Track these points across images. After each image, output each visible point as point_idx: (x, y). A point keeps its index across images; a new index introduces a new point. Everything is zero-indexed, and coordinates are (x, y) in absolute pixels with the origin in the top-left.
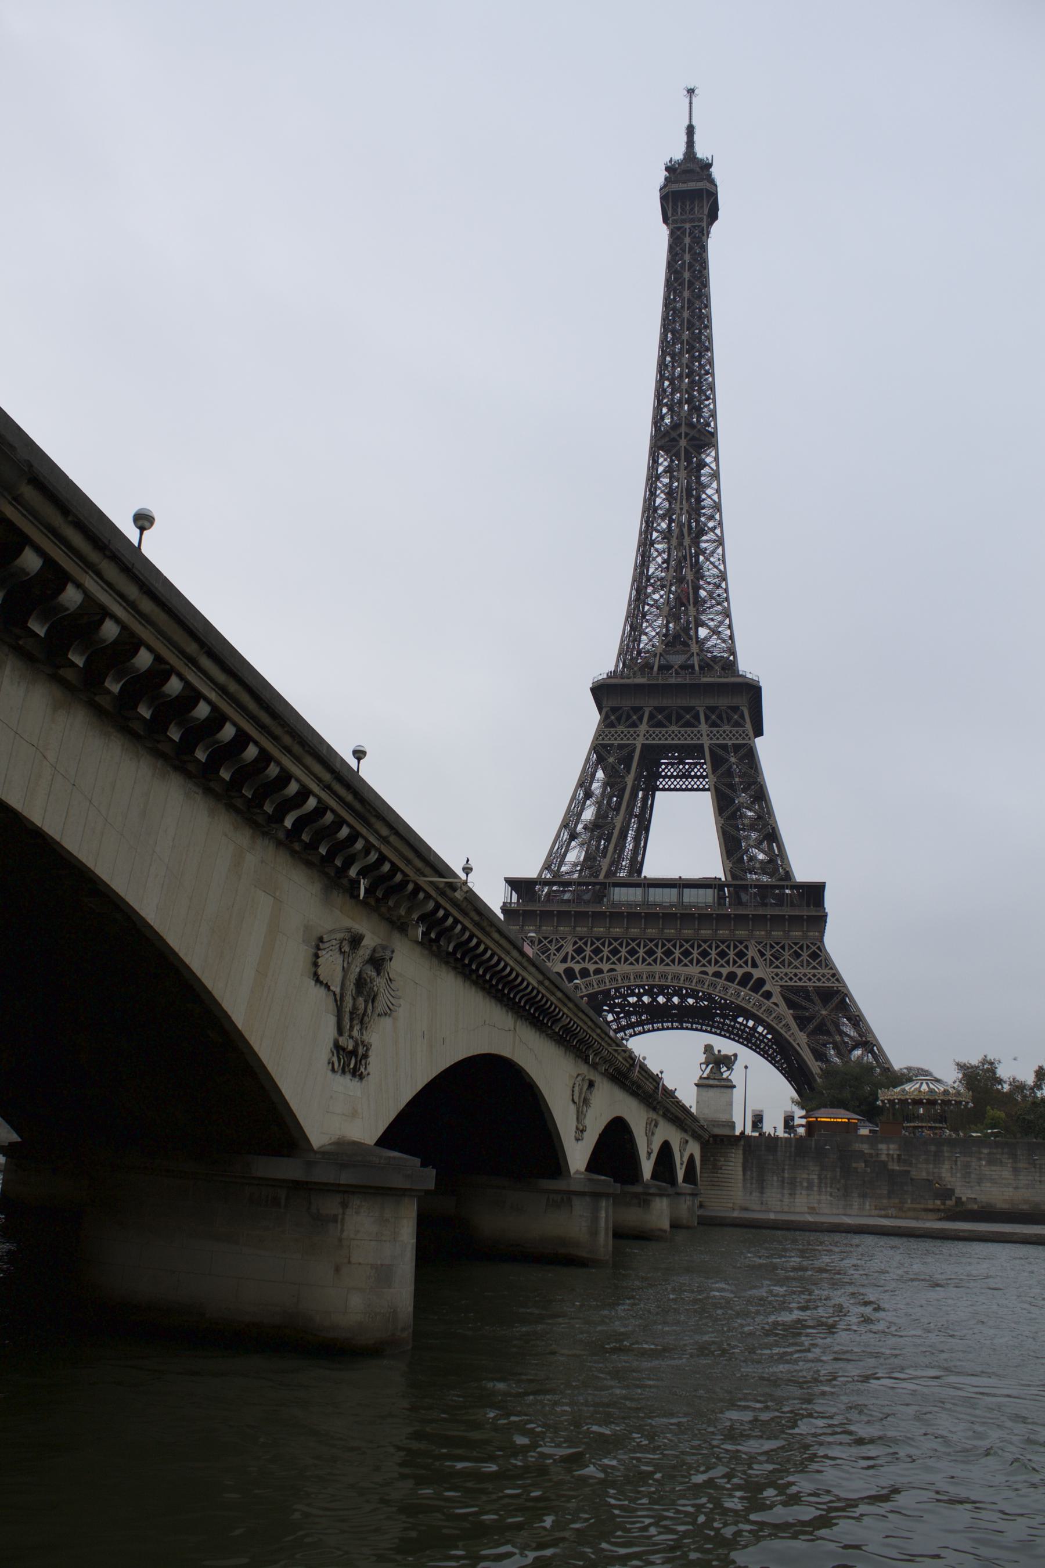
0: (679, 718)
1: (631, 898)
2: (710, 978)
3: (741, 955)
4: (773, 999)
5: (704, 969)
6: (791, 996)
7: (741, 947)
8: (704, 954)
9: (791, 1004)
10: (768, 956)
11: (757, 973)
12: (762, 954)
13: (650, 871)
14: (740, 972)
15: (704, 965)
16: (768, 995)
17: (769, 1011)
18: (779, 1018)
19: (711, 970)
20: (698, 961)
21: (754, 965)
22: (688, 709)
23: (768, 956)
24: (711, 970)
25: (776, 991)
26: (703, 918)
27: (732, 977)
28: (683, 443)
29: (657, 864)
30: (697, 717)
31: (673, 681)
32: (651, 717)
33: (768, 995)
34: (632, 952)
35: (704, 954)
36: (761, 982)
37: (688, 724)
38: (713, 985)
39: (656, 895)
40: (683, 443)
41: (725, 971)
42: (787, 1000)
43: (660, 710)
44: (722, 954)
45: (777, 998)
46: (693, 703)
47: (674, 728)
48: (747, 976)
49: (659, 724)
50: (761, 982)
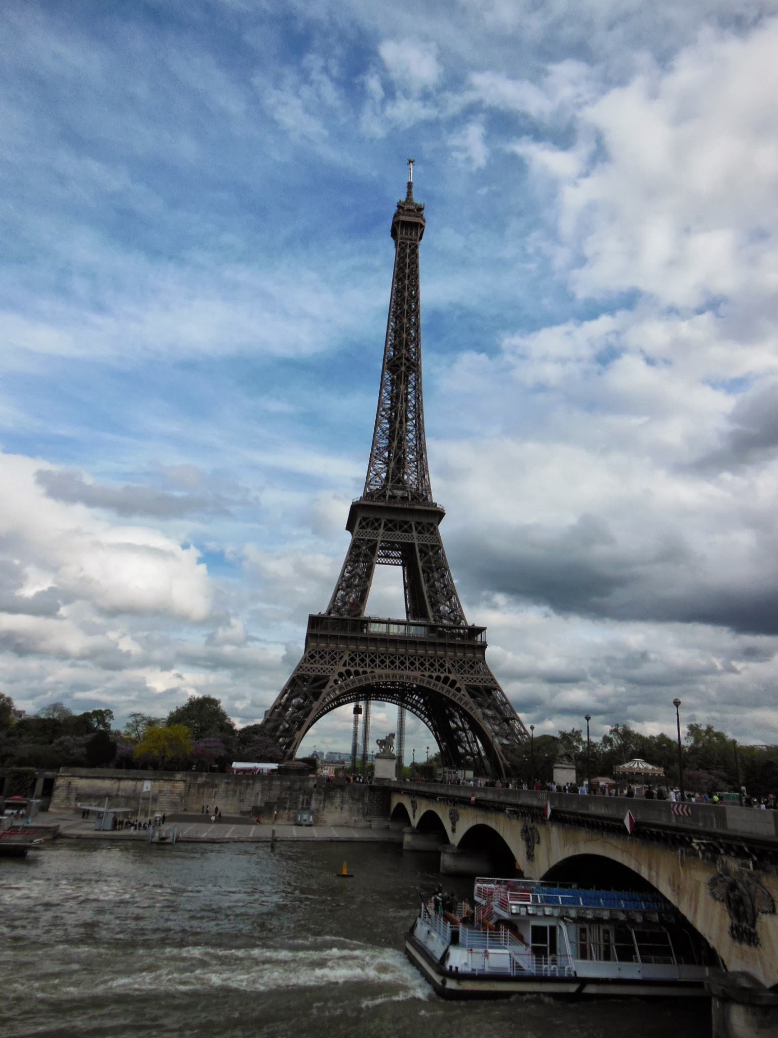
0: (401, 527)
1: (380, 630)
2: (426, 679)
3: (442, 666)
4: (462, 692)
7: (441, 661)
8: (422, 664)
10: (457, 666)
11: (452, 677)
12: (454, 666)
13: (403, 617)
14: (443, 676)
16: (459, 690)
17: (461, 699)
18: (466, 703)
19: (427, 674)
21: (450, 672)
22: (406, 523)
23: (457, 666)
24: (427, 674)
26: (423, 644)
27: (438, 678)
28: (403, 368)
29: (369, 610)
30: (410, 527)
31: (396, 505)
32: (386, 525)
33: (459, 690)
34: (382, 662)
35: (422, 664)
36: (454, 683)
37: (405, 531)
38: (429, 683)
39: (375, 629)
40: (403, 368)
41: (435, 675)
43: (390, 521)
44: (432, 665)
46: (408, 519)
47: (398, 532)
48: (447, 678)
49: (390, 530)
50: (454, 683)
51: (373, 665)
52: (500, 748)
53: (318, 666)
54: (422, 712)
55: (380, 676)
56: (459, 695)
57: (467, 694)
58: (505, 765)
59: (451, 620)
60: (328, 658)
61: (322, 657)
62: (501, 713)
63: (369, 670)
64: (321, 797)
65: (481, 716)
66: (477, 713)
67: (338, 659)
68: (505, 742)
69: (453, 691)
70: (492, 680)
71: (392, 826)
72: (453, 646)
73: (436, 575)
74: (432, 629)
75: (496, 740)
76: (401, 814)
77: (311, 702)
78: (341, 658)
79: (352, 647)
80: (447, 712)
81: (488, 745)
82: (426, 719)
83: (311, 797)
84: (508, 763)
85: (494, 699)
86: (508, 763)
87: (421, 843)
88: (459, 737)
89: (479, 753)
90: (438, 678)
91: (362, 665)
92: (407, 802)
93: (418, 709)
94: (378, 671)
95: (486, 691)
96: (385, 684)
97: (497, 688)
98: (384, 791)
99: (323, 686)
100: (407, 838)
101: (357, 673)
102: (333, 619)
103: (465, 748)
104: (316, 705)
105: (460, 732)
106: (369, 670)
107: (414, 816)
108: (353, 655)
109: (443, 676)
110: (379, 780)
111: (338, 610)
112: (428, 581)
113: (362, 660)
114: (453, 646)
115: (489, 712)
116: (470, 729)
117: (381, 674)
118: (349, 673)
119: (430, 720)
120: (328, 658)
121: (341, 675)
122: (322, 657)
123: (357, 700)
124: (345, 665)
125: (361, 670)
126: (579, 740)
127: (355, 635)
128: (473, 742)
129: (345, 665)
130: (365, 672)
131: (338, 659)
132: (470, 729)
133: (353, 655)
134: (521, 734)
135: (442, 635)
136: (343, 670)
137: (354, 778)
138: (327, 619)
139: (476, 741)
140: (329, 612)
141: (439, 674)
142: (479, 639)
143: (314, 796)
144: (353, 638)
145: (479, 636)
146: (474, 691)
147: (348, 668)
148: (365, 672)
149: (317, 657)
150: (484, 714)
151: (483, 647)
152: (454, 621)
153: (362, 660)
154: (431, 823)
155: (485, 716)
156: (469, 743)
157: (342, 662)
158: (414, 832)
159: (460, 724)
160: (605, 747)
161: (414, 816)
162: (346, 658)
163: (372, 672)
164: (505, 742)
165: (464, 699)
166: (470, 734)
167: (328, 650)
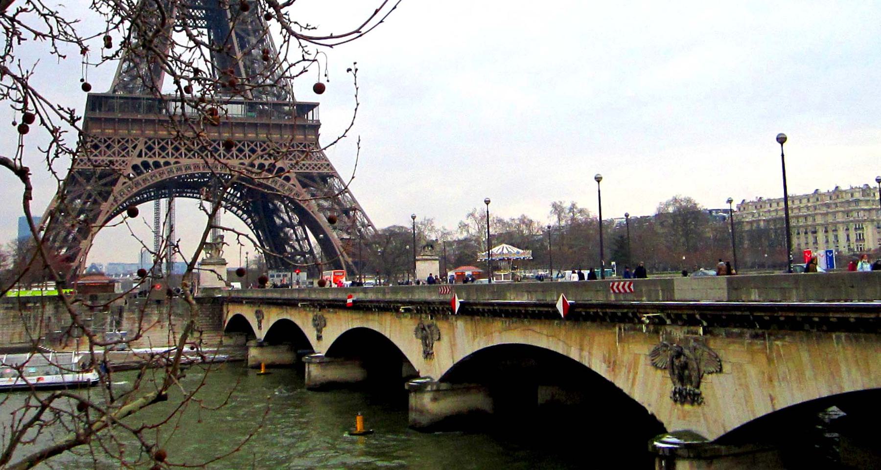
4: (292, 182)
5: (241, 161)
6: (303, 179)
9: (304, 186)
11: (279, 164)
14: (267, 163)
15: (241, 159)
17: (291, 190)
18: (297, 195)
19: (247, 161)
20: (237, 156)
24: (247, 161)
25: (292, 175)
26: (240, 125)
27: (261, 166)
36: (281, 170)
41: (257, 163)
42: (300, 181)
45: (293, 181)
51: (177, 154)
52: (340, 243)
53: (104, 158)
54: (239, 208)
55: (188, 168)
56: (288, 185)
57: (298, 184)
58: (346, 262)
59: (274, 95)
60: (117, 147)
61: (108, 147)
62: (339, 203)
63: (172, 160)
64: (136, 316)
65: (316, 209)
66: (312, 206)
67: (130, 149)
68: (346, 236)
69: (281, 180)
70: (328, 165)
71: (226, 341)
72: (279, 127)
73: (254, 41)
74: (251, 106)
75: (335, 234)
76: (240, 326)
77: (100, 204)
78: (134, 147)
79: (150, 132)
80: (271, 206)
81: (325, 243)
82: (245, 216)
83: (121, 316)
84: (350, 260)
85: (331, 188)
86: (350, 260)
87: (281, 355)
88: (286, 234)
89: (311, 252)
90: (261, 166)
91: (164, 154)
92: (249, 314)
93: (233, 204)
94: (184, 161)
95: (321, 179)
96: (192, 176)
97: (333, 175)
98: (214, 303)
99: (114, 182)
100: (254, 353)
101: (157, 165)
102: (121, 98)
103: (292, 247)
104: (105, 206)
105: (287, 229)
106: (172, 160)
107: (260, 328)
108: (150, 143)
109: (267, 163)
110: (206, 290)
111: (125, 87)
112: (242, 47)
113: (163, 149)
114: (279, 127)
115: (326, 204)
116: (300, 224)
117: (189, 164)
118: (146, 165)
119: (249, 216)
120: (117, 147)
121: (135, 167)
122: (108, 147)
123: (157, 197)
124: (140, 155)
125: (162, 161)
126: (432, 229)
127: (152, 117)
128: (303, 239)
129: (140, 155)
130: (167, 164)
131: (130, 149)
132: (300, 224)
133: (150, 143)
134: (363, 225)
135: (262, 113)
136: (138, 161)
137: (160, 288)
138: (113, 98)
139: (307, 238)
140: (115, 91)
141: (262, 161)
142: (310, 118)
143: (125, 315)
144: (148, 121)
145: (310, 113)
146: (307, 180)
147: (144, 159)
148: (167, 164)
149: (103, 147)
150: (318, 205)
151: (316, 127)
152: (278, 96)
153: (163, 149)
154: (286, 335)
155: (321, 208)
156: (298, 240)
157: (137, 151)
158: (260, 345)
159: (286, 218)
160: (461, 233)
161: (260, 328)
162: (141, 146)
163: (177, 163)
164: (346, 236)
165: (294, 188)
166: (300, 231)
167: (116, 138)
